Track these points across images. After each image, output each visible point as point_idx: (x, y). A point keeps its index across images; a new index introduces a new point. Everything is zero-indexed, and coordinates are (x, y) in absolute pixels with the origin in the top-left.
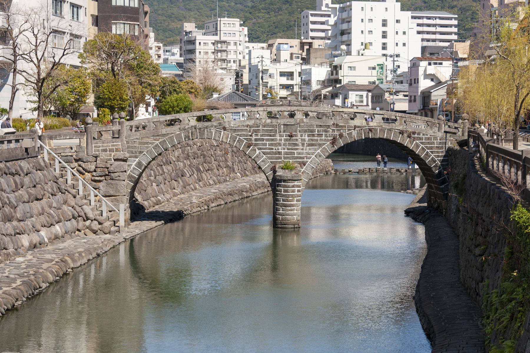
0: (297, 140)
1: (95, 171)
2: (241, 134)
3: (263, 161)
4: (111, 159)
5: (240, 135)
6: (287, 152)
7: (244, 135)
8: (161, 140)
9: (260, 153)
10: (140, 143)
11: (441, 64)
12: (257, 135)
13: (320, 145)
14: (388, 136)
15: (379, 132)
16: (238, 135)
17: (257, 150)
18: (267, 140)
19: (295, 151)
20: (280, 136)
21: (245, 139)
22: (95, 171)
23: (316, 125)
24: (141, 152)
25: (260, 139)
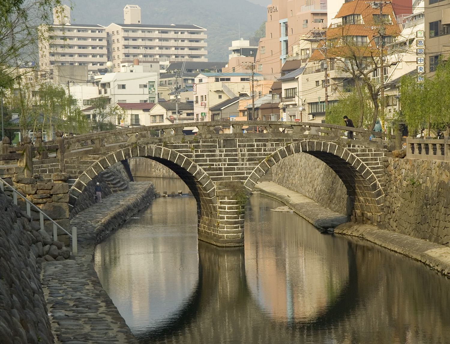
0: (236, 155)
1: (36, 193)
3: (203, 178)
6: (227, 168)
7: (185, 152)
8: (100, 159)
11: (228, 80)
12: (197, 151)
13: (259, 159)
14: (325, 148)
15: (316, 145)
16: (179, 151)
17: (198, 166)
18: (207, 156)
19: (236, 167)
20: (220, 151)
21: (185, 155)
22: (36, 193)
24: (81, 172)
25: (200, 155)
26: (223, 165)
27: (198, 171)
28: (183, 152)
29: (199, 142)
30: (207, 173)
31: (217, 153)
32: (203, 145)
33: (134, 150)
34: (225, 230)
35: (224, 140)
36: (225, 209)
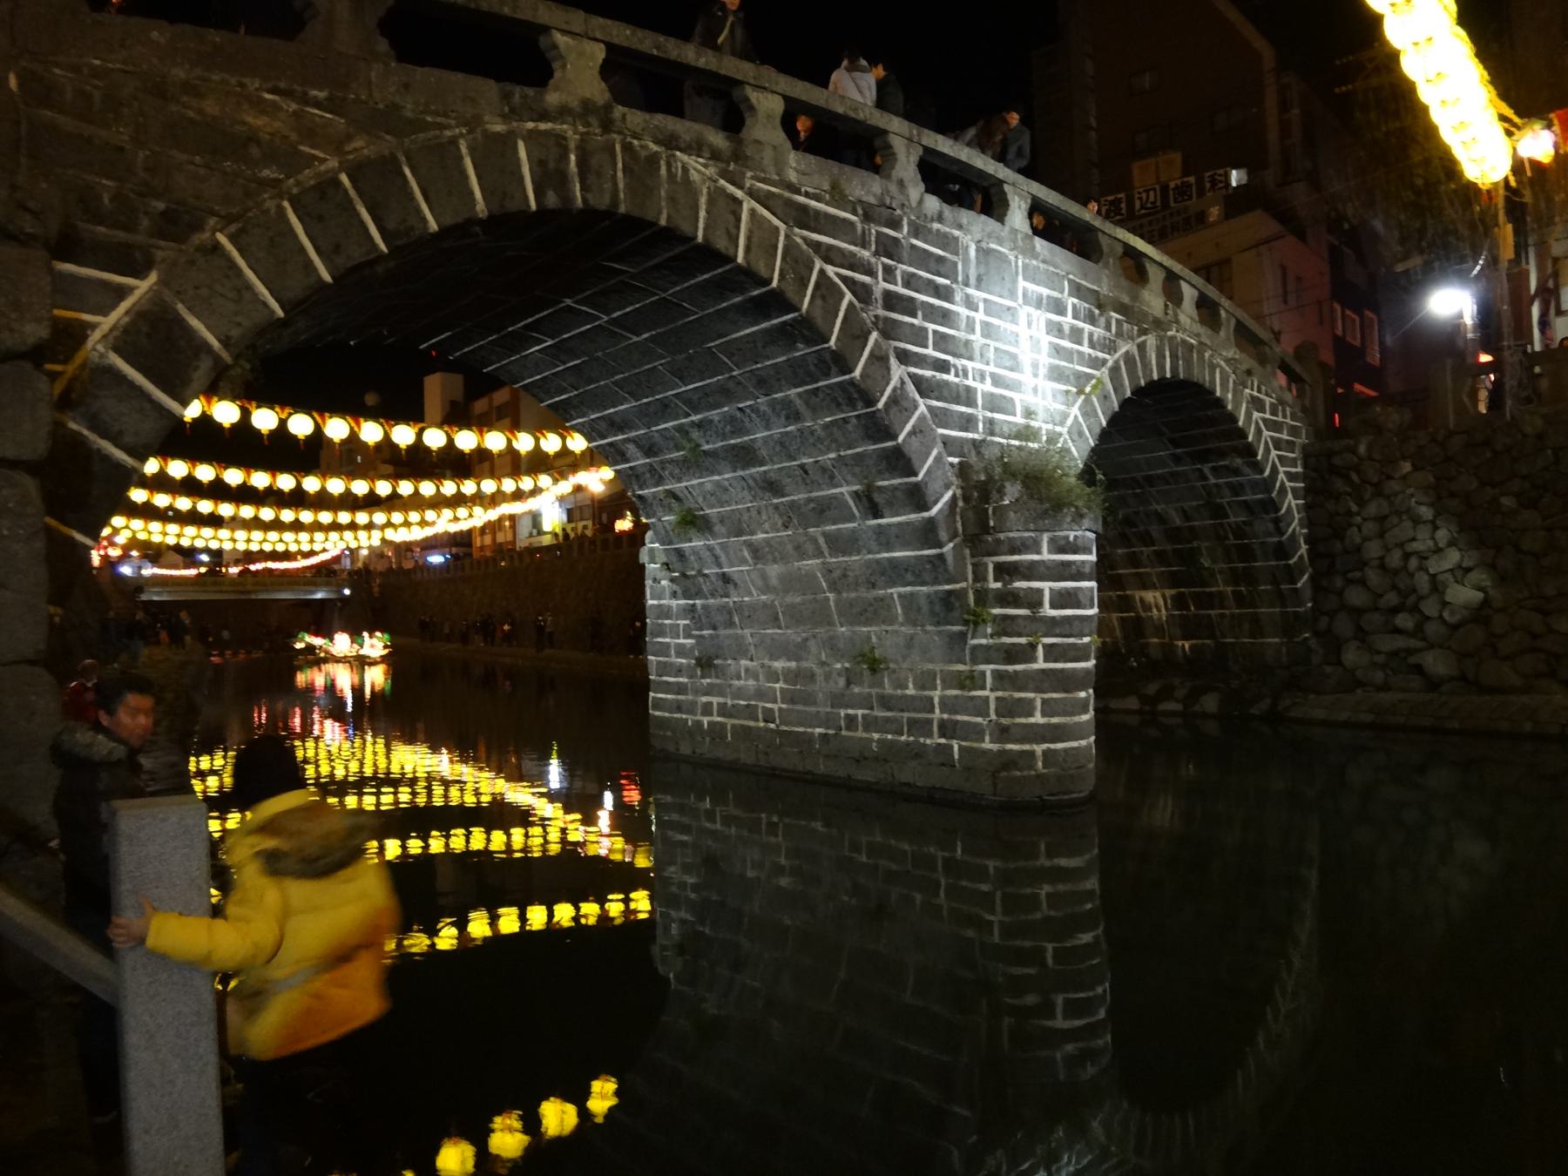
2: (831, 248)
3: (913, 433)
5: (829, 255)
9: (903, 383)
12: (889, 273)
16: (817, 246)
17: (893, 361)
20: (970, 304)
23: (1070, 281)
26: (978, 377)
27: (894, 390)
28: (838, 260)
29: (895, 224)
30: (929, 408)
32: (913, 247)
34: (1038, 718)
35: (978, 250)
36: (1040, 604)
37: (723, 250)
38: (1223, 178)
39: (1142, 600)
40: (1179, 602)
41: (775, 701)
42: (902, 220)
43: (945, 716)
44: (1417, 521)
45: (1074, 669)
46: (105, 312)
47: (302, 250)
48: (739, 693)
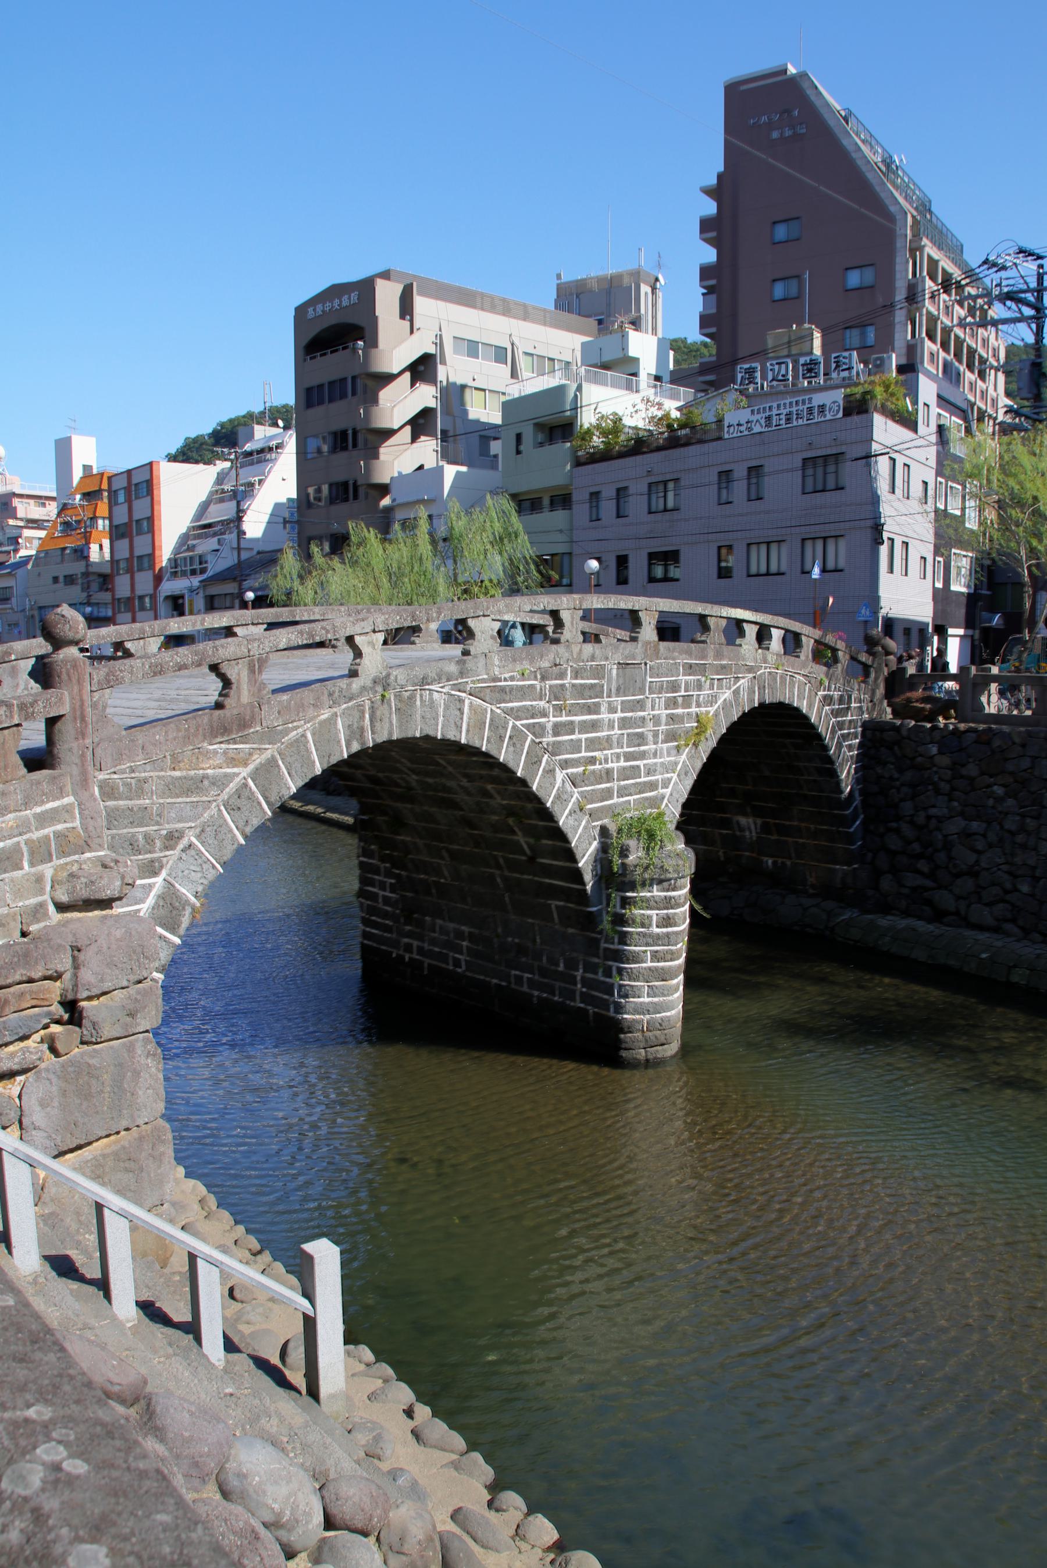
2: (519, 709)
4: (42, 905)
8: (258, 760)
10: (174, 788)
16: (509, 712)
24: (172, 839)
26: (614, 759)
31: (604, 716)
32: (574, 685)
33: (378, 713)
36: (650, 925)
37: (453, 738)
38: (847, 361)
39: (738, 823)
40: (765, 828)
41: (461, 953)
42: (566, 669)
43: (584, 990)
44: (938, 792)
45: (670, 967)
46: (142, 901)
47: (231, 831)
48: (433, 942)
